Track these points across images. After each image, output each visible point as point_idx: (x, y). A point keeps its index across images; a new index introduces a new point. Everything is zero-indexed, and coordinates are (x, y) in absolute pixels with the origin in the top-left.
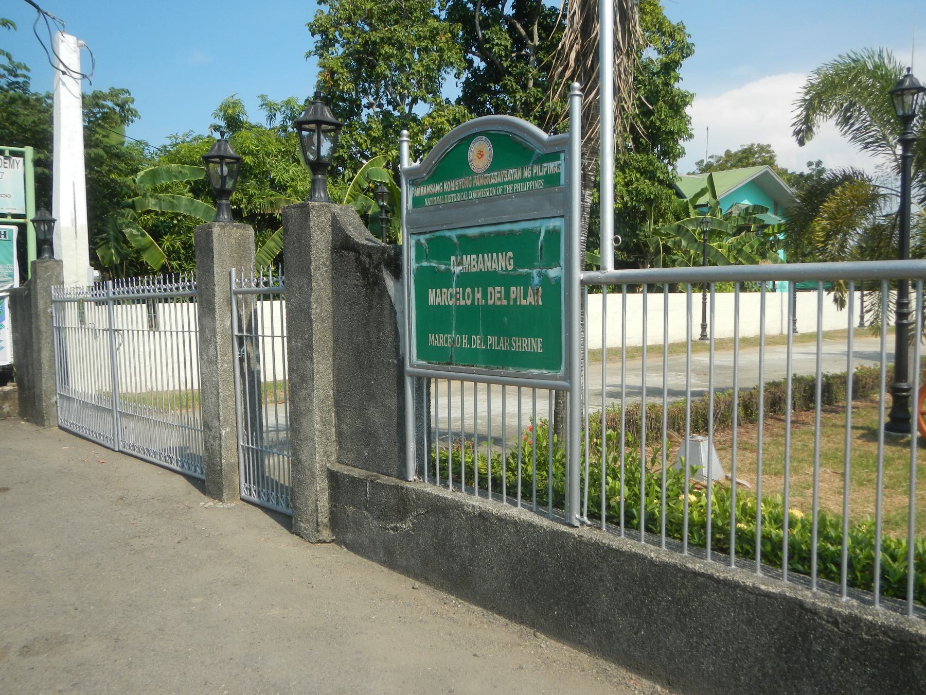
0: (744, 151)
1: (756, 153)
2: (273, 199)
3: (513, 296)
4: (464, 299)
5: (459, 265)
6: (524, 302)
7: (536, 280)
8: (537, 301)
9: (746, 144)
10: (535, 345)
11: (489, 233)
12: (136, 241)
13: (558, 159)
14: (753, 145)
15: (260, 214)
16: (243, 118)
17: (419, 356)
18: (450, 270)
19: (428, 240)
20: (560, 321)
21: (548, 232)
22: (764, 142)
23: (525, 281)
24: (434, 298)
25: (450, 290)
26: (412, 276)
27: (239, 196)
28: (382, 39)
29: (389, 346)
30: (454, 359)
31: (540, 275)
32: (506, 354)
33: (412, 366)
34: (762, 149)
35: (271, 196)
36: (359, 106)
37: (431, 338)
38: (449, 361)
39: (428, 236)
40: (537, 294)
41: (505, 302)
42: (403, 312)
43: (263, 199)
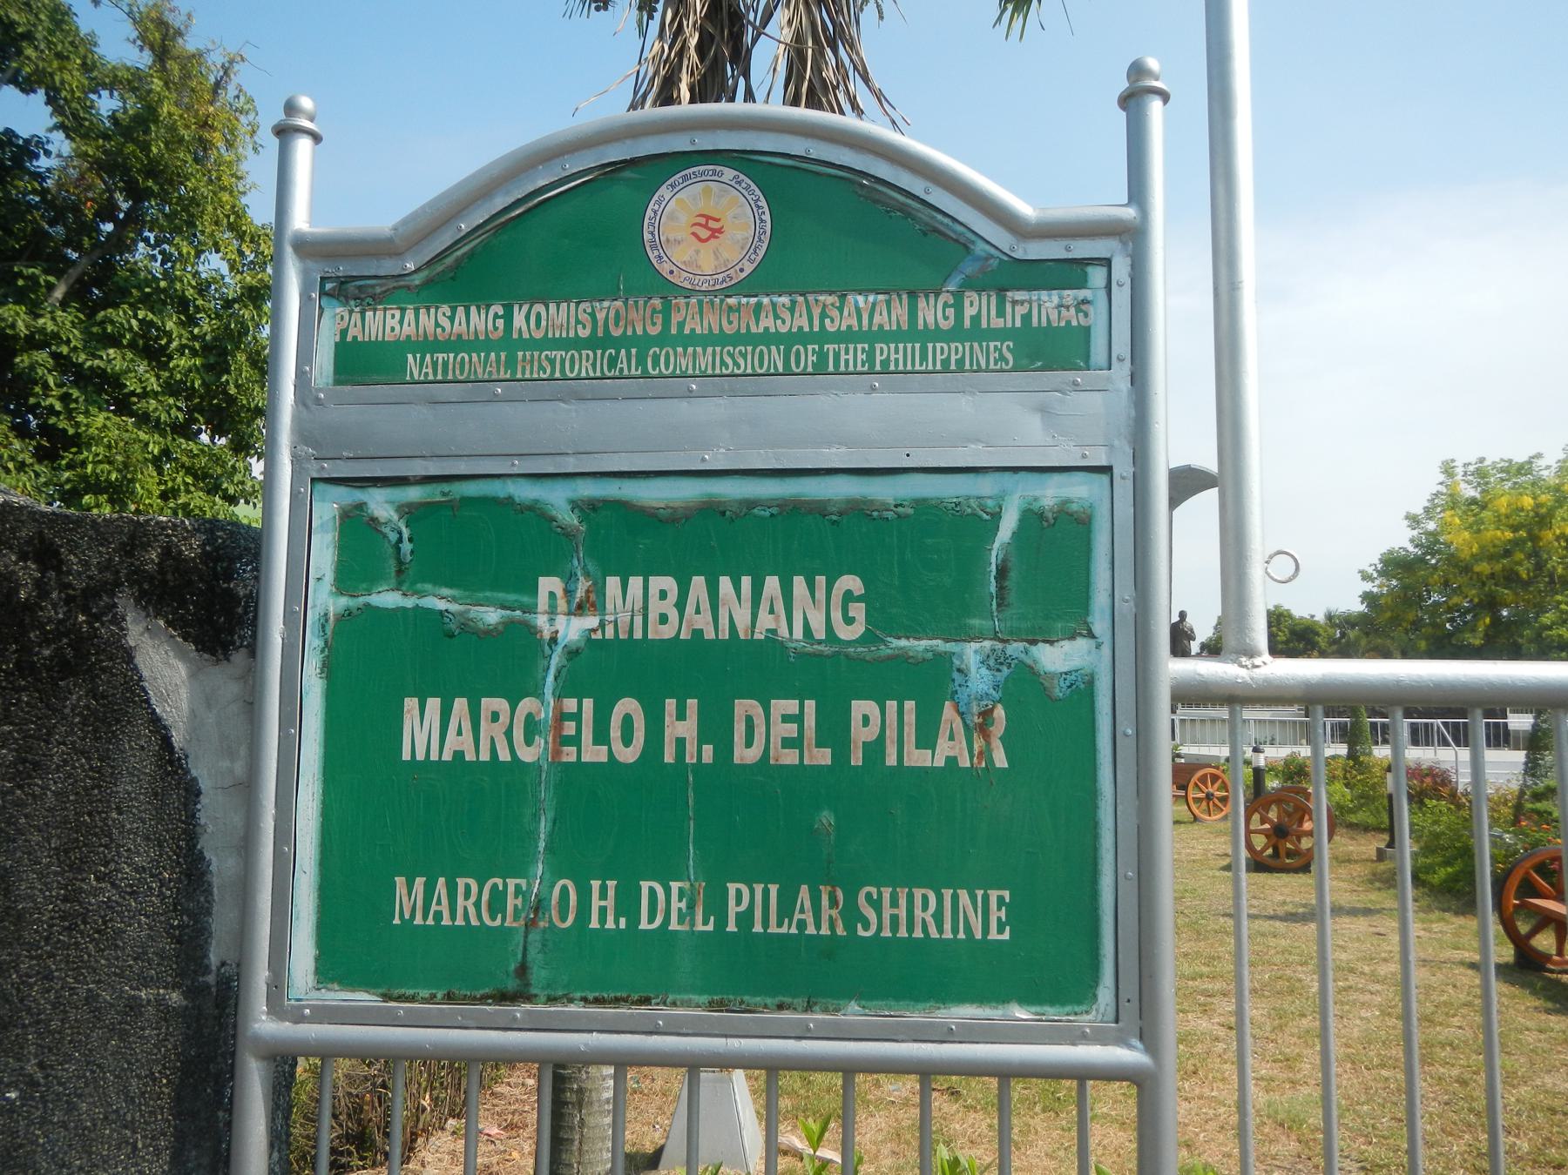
3: (861, 735)
4: (601, 737)
5: (580, 609)
6: (918, 758)
7: (980, 680)
8: (986, 754)
10: (979, 915)
11: (751, 504)
13: (1082, 284)
17: (329, 970)
18: (533, 631)
19: (409, 512)
20: (1095, 825)
21: (1033, 518)
23: (930, 684)
24: (425, 731)
25: (527, 705)
26: (314, 642)
29: (135, 932)
30: (538, 975)
31: (995, 662)
32: (828, 949)
33: (276, 1007)
37: (407, 897)
38: (512, 985)
39: (414, 494)
40: (984, 730)
41: (824, 757)
42: (248, 787)
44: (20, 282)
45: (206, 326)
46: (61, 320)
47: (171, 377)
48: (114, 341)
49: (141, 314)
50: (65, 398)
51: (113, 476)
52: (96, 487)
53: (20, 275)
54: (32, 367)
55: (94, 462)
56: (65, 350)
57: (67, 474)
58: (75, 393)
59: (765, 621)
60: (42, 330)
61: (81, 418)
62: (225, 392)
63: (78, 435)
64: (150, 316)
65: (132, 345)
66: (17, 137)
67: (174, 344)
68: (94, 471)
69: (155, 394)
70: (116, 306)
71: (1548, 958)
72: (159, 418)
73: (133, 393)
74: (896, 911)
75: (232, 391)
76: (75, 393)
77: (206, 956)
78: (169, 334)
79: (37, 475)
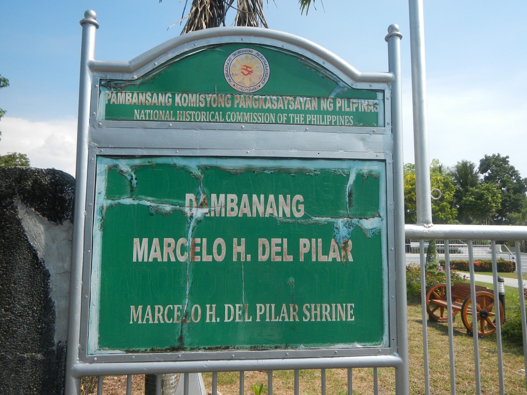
0: (10, 156)
1: (17, 158)
3: (303, 251)
4: (210, 252)
5: (201, 206)
6: (323, 258)
7: (343, 231)
8: (346, 257)
9: (11, 152)
10: (344, 313)
11: (265, 169)
13: (375, 98)
14: (15, 153)
17: (103, 343)
18: (184, 213)
19: (136, 169)
20: (382, 280)
21: (360, 176)
22: (22, 153)
23: (327, 233)
24: (141, 250)
25: (181, 241)
26: (97, 217)
29: (22, 331)
30: (187, 340)
31: (349, 225)
32: (292, 327)
33: (83, 358)
34: (22, 156)
37: (136, 313)
38: (177, 344)
39: (137, 162)
40: (345, 248)
41: (290, 258)
42: (71, 273)
59: (269, 210)
71: (438, 318)
74: (316, 312)
77: (53, 339)
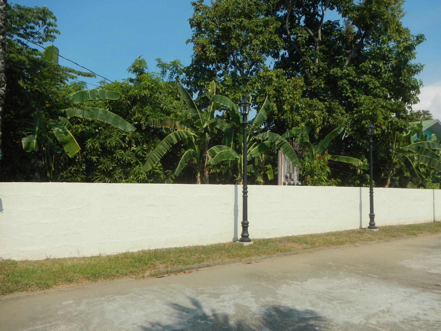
2: (162, 118)
12: (60, 137)
15: (153, 128)
16: (146, 71)
27: (140, 116)
28: (234, 26)
35: (161, 116)
36: (215, 75)
43: (156, 118)
44: (338, 61)
45: (393, 62)
46: (348, 69)
47: (383, 81)
48: (365, 73)
49: (372, 62)
50: (352, 93)
51: (370, 113)
52: (365, 117)
53: (337, 59)
54: (343, 85)
55: (364, 110)
56: (351, 78)
57: (356, 115)
58: (355, 90)
60: (344, 73)
61: (357, 98)
62: (401, 83)
63: (357, 103)
64: (375, 62)
65: (370, 73)
66: (331, 22)
67: (383, 70)
68: (364, 112)
69: (379, 87)
70: (365, 62)
72: (380, 95)
73: (371, 88)
75: (403, 82)
76: (355, 90)
78: (380, 68)
79: (347, 117)
